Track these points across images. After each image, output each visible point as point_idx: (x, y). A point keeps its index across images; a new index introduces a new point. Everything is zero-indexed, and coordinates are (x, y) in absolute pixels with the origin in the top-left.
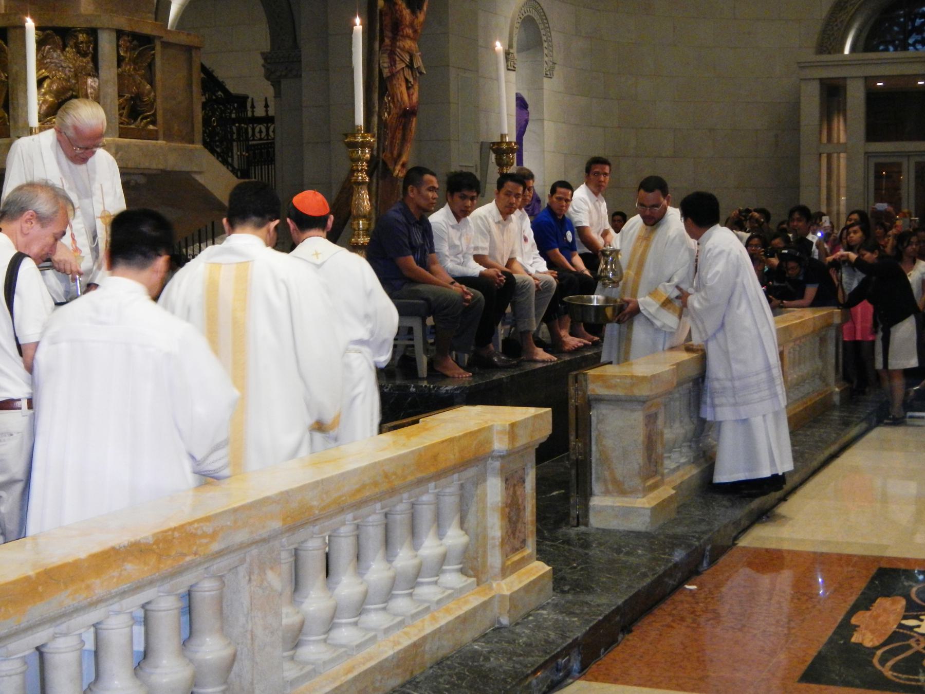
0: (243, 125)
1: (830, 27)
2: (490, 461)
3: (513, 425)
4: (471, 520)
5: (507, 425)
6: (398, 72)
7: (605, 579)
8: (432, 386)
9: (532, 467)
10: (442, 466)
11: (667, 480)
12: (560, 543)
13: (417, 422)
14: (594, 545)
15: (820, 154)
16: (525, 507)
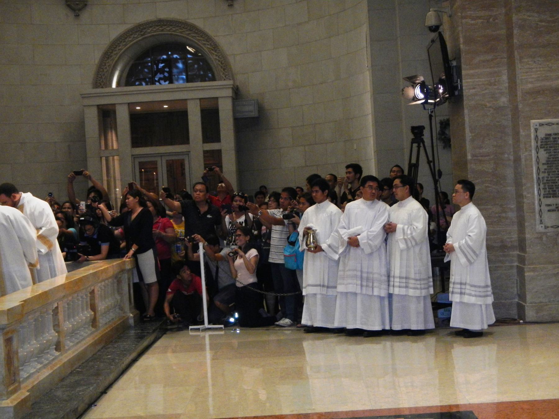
11: (23, 386)
15: (101, 158)
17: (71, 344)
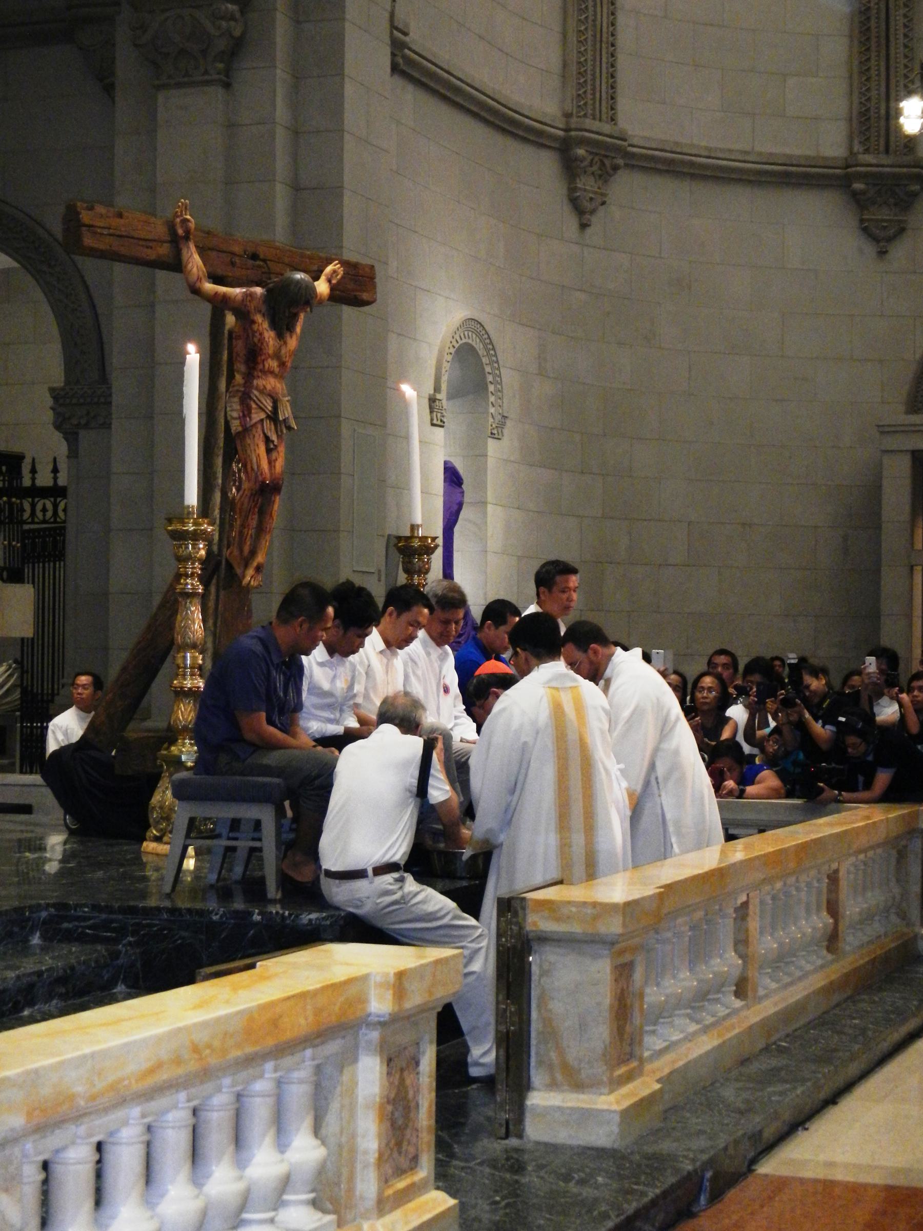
0: (14, 500)
2: (364, 1030)
3: (400, 975)
4: (332, 1123)
6: (255, 425)
7: (542, 1222)
8: (287, 913)
9: (431, 1042)
10: (288, 1035)
11: (648, 1067)
13: (252, 966)
14: (530, 1168)
15: (912, 568)
16: (417, 1105)
17: (774, 985)
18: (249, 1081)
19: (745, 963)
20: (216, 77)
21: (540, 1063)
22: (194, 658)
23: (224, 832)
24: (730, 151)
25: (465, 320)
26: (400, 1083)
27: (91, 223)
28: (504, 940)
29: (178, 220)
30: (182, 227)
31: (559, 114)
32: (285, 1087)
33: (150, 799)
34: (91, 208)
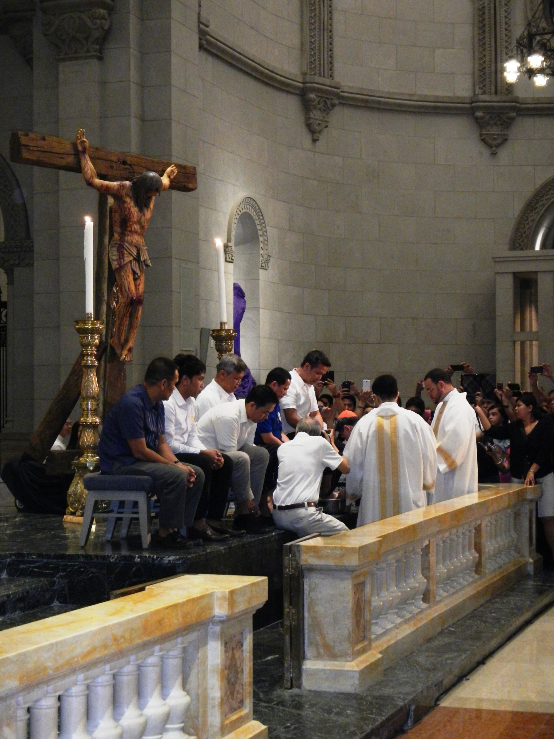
1: (522, 226)
2: (211, 626)
3: (232, 593)
5: (227, 592)
6: (127, 263)
8: (155, 557)
10: (168, 630)
11: (374, 645)
12: (274, 705)
13: (143, 589)
14: (307, 706)
15: (514, 342)
17: (445, 594)
18: (145, 658)
19: (428, 580)
20: (95, 54)
21: (311, 643)
22: (92, 404)
23: (116, 509)
24: (402, 94)
25: (245, 199)
26: (232, 657)
27: (26, 144)
28: (287, 570)
29: (79, 141)
30: (81, 146)
31: (299, 73)
32: (165, 660)
33: (68, 490)
34: (27, 135)
